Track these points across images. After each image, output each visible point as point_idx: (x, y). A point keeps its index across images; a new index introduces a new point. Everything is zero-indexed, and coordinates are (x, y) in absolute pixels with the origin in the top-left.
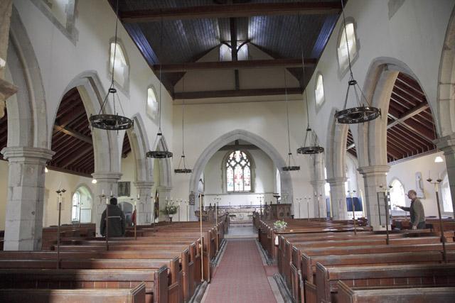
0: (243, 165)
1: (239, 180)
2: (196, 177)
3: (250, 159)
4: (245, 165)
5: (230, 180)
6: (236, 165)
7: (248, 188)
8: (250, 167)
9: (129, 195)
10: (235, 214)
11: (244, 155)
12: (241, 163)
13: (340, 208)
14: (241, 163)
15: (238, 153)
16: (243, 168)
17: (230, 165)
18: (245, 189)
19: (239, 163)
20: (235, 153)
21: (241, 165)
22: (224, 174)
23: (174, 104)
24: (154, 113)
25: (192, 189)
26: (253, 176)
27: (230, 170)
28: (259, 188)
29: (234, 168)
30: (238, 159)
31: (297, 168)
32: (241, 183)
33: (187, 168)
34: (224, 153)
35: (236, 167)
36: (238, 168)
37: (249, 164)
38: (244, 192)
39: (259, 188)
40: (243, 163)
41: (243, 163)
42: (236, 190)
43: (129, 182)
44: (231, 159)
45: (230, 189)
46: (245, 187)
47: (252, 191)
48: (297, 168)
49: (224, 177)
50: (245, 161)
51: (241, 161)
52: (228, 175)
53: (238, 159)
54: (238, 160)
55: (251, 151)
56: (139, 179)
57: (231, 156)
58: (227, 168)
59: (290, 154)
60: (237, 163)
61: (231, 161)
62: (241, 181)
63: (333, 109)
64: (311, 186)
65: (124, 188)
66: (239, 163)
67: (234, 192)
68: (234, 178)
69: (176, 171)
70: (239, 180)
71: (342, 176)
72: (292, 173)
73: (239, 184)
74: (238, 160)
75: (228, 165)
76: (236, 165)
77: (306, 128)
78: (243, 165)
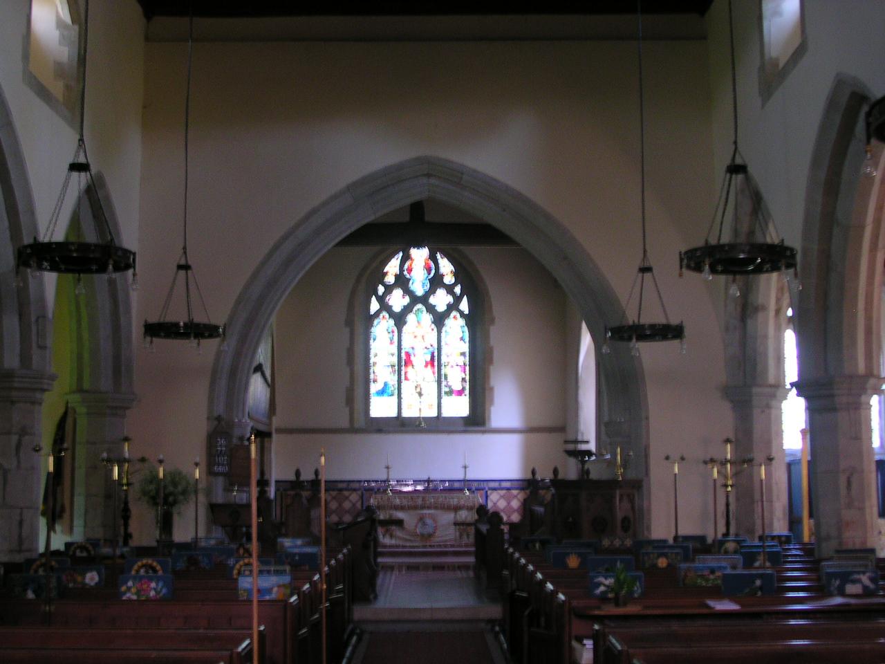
0: (441, 308)
1: (420, 374)
2: (238, 354)
4: (452, 307)
6: (407, 309)
7: (458, 407)
8: (474, 321)
10: (400, 515)
11: (446, 267)
12: (432, 300)
13: (849, 505)
14: (432, 300)
15: (420, 255)
16: (439, 320)
17: (385, 307)
18: (446, 413)
20: (406, 257)
21: (431, 309)
22: (358, 348)
23: (147, 39)
24: (60, 71)
25: (220, 409)
27: (382, 329)
29: (400, 320)
30: (419, 284)
31: (671, 332)
32: (431, 389)
33: (199, 318)
34: (363, 253)
35: (411, 318)
36: (419, 323)
37: (464, 306)
38: (439, 425)
40: (441, 300)
41: (441, 300)
44: (390, 279)
45: (381, 408)
46: (445, 399)
47: (476, 420)
48: (671, 332)
50: (450, 289)
51: (432, 291)
52: (374, 347)
53: (419, 284)
54: (419, 287)
55: (476, 253)
57: (392, 268)
58: (370, 319)
59: (645, 270)
60: (415, 300)
61: (389, 289)
62: (429, 375)
63: (840, 83)
66: (424, 300)
67: (401, 425)
68: (403, 362)
69: (154, 330)
70: (420, 374)
71: (861, 368)
72: (649, 353)
74: (419, 290)
75: (374, 306)
76: (407, 309)
77: (728, 162)
78: (441, 308)
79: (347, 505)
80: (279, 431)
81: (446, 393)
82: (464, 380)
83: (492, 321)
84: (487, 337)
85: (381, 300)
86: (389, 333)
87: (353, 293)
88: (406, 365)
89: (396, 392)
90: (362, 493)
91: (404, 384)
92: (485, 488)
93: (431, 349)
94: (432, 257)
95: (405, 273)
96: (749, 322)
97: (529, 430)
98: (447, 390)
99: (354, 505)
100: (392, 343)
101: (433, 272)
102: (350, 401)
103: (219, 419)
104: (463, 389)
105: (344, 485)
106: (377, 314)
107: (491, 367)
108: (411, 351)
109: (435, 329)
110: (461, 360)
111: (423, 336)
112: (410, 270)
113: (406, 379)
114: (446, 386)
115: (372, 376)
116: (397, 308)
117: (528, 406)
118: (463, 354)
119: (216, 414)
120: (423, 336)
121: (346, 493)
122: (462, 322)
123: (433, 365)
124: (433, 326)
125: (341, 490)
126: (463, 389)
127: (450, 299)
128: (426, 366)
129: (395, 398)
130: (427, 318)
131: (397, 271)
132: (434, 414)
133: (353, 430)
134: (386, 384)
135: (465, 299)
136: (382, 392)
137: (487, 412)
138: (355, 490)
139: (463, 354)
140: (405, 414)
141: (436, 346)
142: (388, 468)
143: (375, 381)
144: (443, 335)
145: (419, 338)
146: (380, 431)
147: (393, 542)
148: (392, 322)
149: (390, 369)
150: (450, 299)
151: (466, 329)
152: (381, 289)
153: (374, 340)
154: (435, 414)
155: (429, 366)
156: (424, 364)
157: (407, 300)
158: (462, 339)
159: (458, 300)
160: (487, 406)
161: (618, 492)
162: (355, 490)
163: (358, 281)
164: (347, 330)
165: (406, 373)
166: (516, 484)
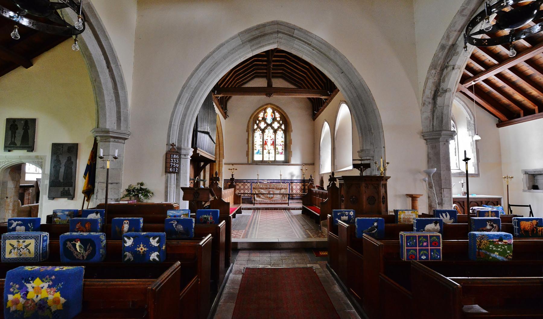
0: (276, 127)
1: (269, 147)
3: (285, 120)
4: (279, 127)
6: (266, 128)
8: (286, 132)
9: (31, 148)
11: (278, 115)
12: (273, 125)
14: (273, 125)
16: (275, 131)
17: (259, 127)
18: (277, 159)
19: (270, 125)
20: (265, 112)
21: (273, 128)
22: (250, 139)
25: (174, 140)
26: (288, 142)
27: (258, 134)
28: (296, 158)
29: (263, 131)
32: (272, 151)
35: (266, 131)
36: (269, 132)
37: (283, 127)
38: (275, 163)
39: (296, 158)
40: (276, 125)
41: (276, 125)
42: (266, 159)
43: (34, 121)
44: (260, 119)
45: (257, 157)
46: (277, 155)
47: (287, 162)
49: (250, 142)
50: (279, 122)
51: (273, 122)
54: (269, 121)
56: (100, 126)
57: (261, 115)
58: (254, 131)
60: (268, 125)
61: (260, 121)
62: (272, 148)
64: (423, 142)
65: (20, 132)
66: (270, 125)
67: (263, 163)
68: (264, 144)
70: (269, 147)
73: (269, 153)
74: (269, 121)
75: (256, 127)
76: (266, 128)
78: (276, 127)
80: (225, 164)
81: (277, 153)
82: (282, 149)
83: (292, 132)
84: (290, 136)
85: (257, 125)
87: (249, 121)
88: (265, 145)
89: (262, 153)
91: (265, 151)
93: (273, 140)
94: (273, 112)
95: (265, 117)
96: (439, 100)
97: (303, 164)
98: (278, 152)
101: (273, 117)
102: (248, 155)
103: (173, 145)
104: (282, 152)
105: (246, 181)
106: (256, 129)
107: (291, 145)
108: (267, 141)
109: (274, 134)
111: (270, 136)
112: (267, 116)
113: (265, 149)
115: (255, 148)
116: (263, 127)
117: (303, 158)
118: (282, 142)
119: (171, 143)
120: (270, 136)
121: (246, 183)
122: (282, 132)
123: (273, 145)
124: (273, 133)
125: (244, 182)
126: (282, 152)
127: (279, 125)
128: (271, 145)
129: (262, 155)
130: (272, 131)
131: (262, 116)
132: (273, 159)
133: (248, 164)
135: (283, 125)
136: (258, 153)
137: (290, 159)
138: (249, 182)
139: (282, 142)
140: (265, 159)
141: (274, 139)
144: (277, 136)
145: (269, 137)
146: (257, 164)
147: (260, 199)
148: (261, 132)
149: (260, 146)
150: (279, 125)
151: (283, 134)
152: (258, 122)
153: (256, 137)
154: (274, 160)
156: (270, 144)
157: (266, 125)
158: (282, 137)
159: (281, 125)
162: (249, 182)
163: (250, 118)
164: (247, 133)
165: (265, 147)
166: (299, 181)
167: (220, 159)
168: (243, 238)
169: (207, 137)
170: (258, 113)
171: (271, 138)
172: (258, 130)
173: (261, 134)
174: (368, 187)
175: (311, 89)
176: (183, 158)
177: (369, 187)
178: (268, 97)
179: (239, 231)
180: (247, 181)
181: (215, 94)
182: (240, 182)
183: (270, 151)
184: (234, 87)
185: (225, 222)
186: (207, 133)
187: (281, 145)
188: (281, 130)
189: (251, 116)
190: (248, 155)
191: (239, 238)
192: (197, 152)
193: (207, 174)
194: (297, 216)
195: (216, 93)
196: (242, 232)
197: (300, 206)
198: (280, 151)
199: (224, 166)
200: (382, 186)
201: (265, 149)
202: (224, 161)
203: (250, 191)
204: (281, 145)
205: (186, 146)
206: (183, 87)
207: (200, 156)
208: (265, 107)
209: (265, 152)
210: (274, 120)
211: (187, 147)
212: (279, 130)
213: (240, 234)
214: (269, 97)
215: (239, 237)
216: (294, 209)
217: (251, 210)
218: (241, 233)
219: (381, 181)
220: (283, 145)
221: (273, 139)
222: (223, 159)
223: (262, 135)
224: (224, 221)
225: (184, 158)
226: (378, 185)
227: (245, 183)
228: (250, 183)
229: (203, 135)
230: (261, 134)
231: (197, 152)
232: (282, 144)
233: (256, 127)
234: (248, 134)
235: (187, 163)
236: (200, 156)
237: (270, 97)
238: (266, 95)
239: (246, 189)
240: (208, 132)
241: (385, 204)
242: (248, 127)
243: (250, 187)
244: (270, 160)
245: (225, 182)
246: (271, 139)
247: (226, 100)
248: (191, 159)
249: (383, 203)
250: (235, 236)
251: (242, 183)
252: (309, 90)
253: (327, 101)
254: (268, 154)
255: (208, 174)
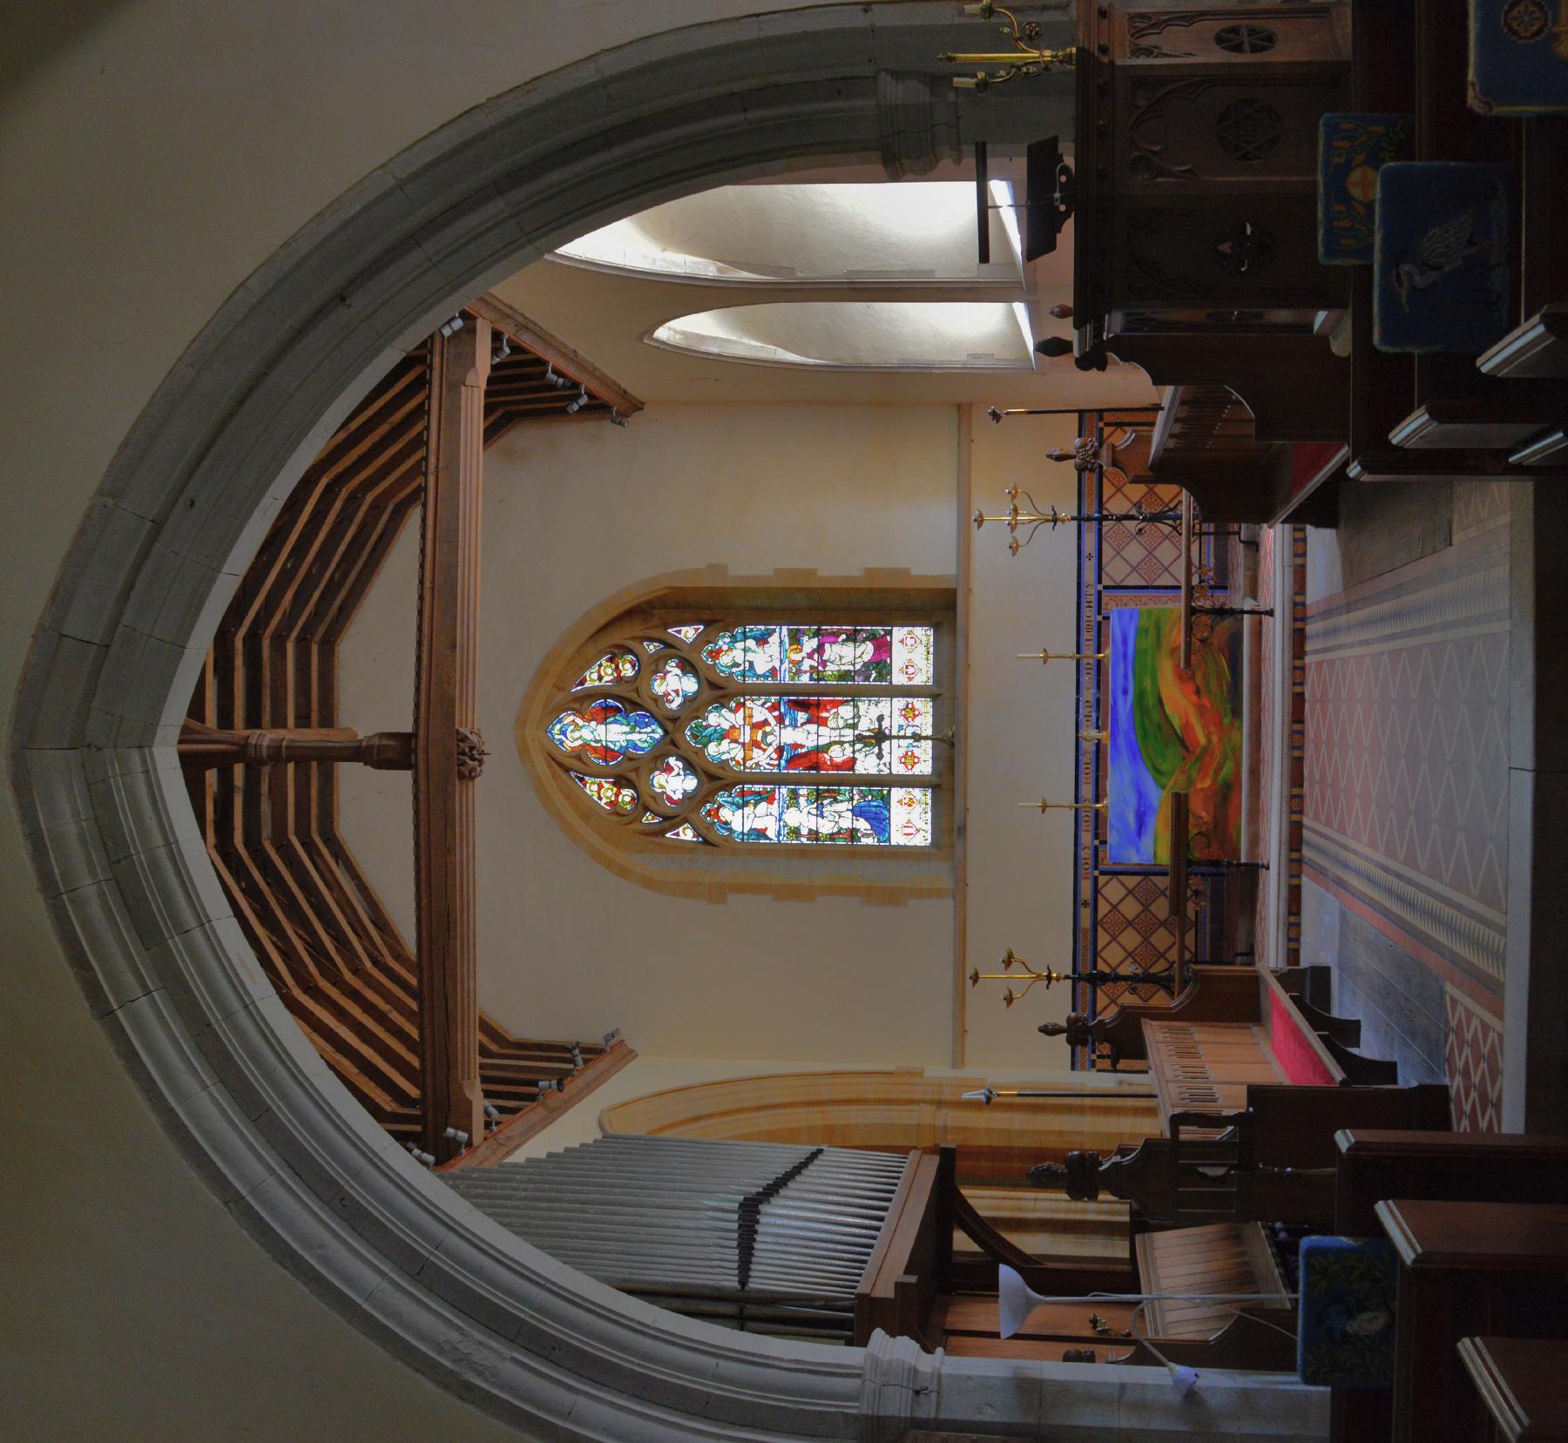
4: (688, 667)
5: (839, 817)
16: (720, 691)
18: (923, 675)
19: (671, 723)
21: (695, 706)
27: (738, 819)
32: (870, 713)
37: (688, 633)
44: (627, 795)
46: (898, 679)
50: (656, 666)
54: (647, 736)
60: (670, 745)
73: (879, 737)
78: (690, 685)
79: (1131, 909)
80: (958, 1060)
81: (880, 677)
82: (852, 638)
85: (671, 820)
86: (746, 804)
87: (649, 883)
90: (1102, 873)
91: (860, 768)
92: (1100, 593)
99: (1130, 892)
100: (770, 800)
104: (872, 638)
105: (1086, 914)
110: (810, 644)
114: (867, 678)
118: (795, 639)
121: (1103, 909)
122: (723, 642)
123: (818, 706)
128: (822, 722)
130: (718, 719)
133: (959, 890)
134: (857, 812)
138: (1096, 891)
139: (795, 639)
140: (925, 768)
141: (773, 699)
142: (1044, 808)
143: (853, 834)
148: (722, 797)
150: (672, 667)
152: (648, 818)
155: (824, 714)
156: (812, 727)
159: (671, 648)
160: (910, 585)
161: (1124, 60)
162: (1096, 891)
163: (623, 872)
164: (733, 898)
167: (925, 1102)
168: (1500, 1015)
169: (777, 1217)
170: (588, 810)
171: (766, 723)
172: (709, 813)
173: (742, 794)
174: (1152, 152)
175: (426, 459)
176: (938, 1410)
177: (1156, 149)
178: (481, 762)
179: (1453, 1024)
180: (1086, 904)
181: (469, 1144)
182: (1095, 954)
183: (865, 726)
184: (414, 998)
185: (1385, 1198)
186: (750, 1210)
187: (820, 650)
188: (710, 647)
189: (609, 864)
190: (891, 896)
191: (1501, 1037)
192: (890, 1294)
193: (1034, 1210)
194: (1353, 568)
195: (463, 1135)
196: (1460, 1009)
197: (1274, 537)
198: (867, 650)
199: (969, 1072)
200: (1148, 52)
201: (852, 762)
202: (938, 1070)
203: (1163, 882)
204: (820, 650)
205: (856, 1382)
206: (461, 1397)
207: (913, 1279)
208: (541, 765)
209: (867, 764)
210: (634, 696)
211: (859, 1376)
212: (710, 662)
213: (1475, 1023)
214: (485, 758)
215: (1492, 1035)
216: (1299, 576)
217: (1298, 887)
218: (1470, 1014)
219: (1112, 63)
220: (817, 634)
221: (774, 708)
222: (921, 1074)
223: (747, 787)
224: (1381, 1208)
225: (934, 1396)
226: (1142, 80)
227: (1100, 915)
228: (1102, 879)
229: (763, 1244)
230: (742, 794)
231: (890, 1294)
232: (814, 643)
233: (687, 834)
234: (739, 889)
235: (970, 1378)
236: (913, 1279)
237: (486, 749)
238: (468, 777)
239: (1146, 908)
240: (741, 1205)
241: (1273, 26)
242: (687, 890)
243: (1131, 881)
244: (929, 732)
245: (1093, 1064)
246: (773, 722)
247: (494, 1048)
248: (940, 1350)
249: (1269, 40)
250: (1483, 1066)
251: (1103, 938)
252: (432, 467)
253: (508, 331)
254: (886, 745)
255: (1040, 1205)
